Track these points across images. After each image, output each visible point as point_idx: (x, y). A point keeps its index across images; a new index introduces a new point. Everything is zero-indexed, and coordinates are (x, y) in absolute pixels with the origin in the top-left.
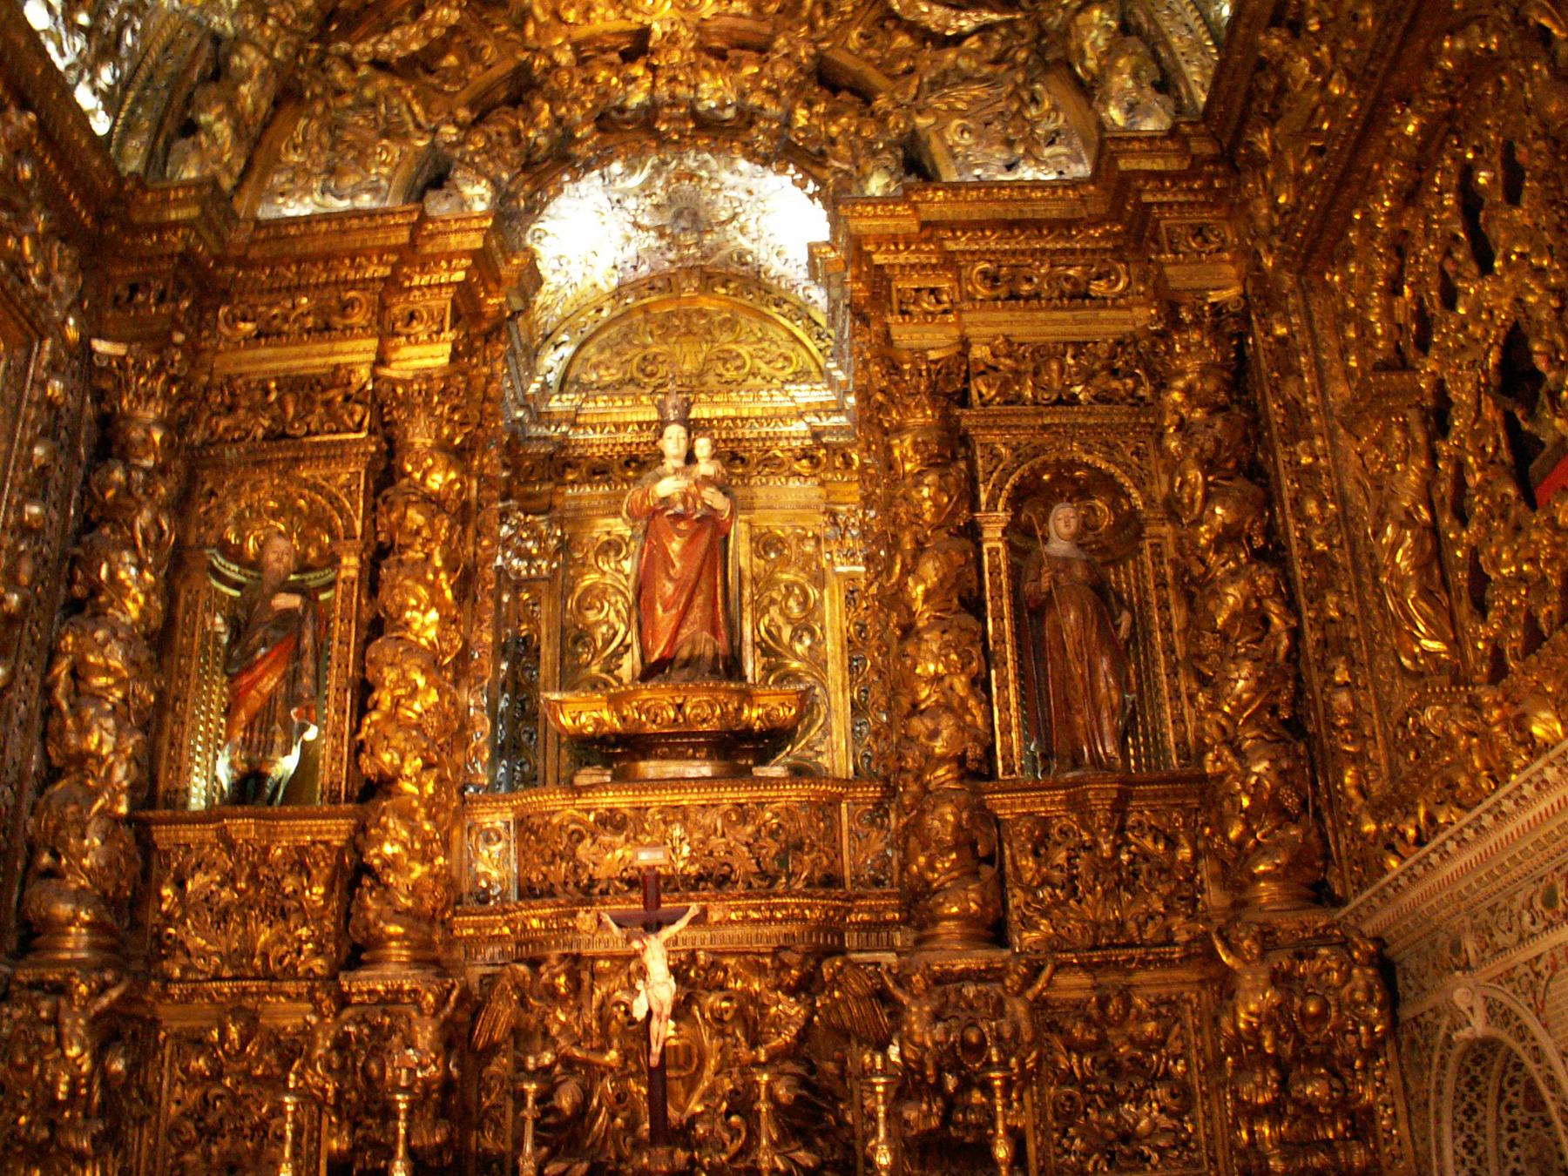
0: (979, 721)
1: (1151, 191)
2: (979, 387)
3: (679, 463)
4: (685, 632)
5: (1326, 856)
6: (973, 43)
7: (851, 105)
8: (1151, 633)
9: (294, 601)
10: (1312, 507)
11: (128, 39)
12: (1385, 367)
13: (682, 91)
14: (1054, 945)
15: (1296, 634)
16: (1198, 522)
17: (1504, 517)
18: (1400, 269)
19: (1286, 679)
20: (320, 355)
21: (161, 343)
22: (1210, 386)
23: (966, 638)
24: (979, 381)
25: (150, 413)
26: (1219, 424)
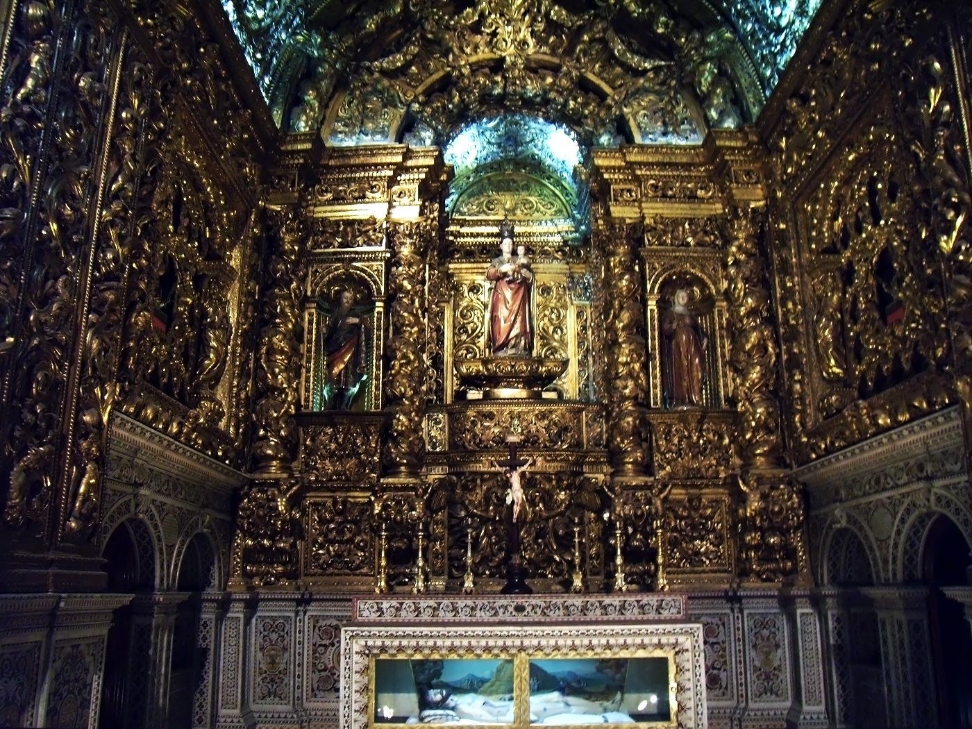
1: (730, 155)
2: (648, 238)
3: (509, 256)
5: (785, 447)
6: (651, 75)
7: (594, 100)
8: (716, 348)
9: (356, 320)
10: (790, 305)
12: (825, 251)
13: (519, 89)
14: (671, 476)
15: (778, 356)
16: (741, 305)
17: (873, 324)
18: (839, 210)
19: (772, 374)
22: (749, 246)
26: (752, 263)
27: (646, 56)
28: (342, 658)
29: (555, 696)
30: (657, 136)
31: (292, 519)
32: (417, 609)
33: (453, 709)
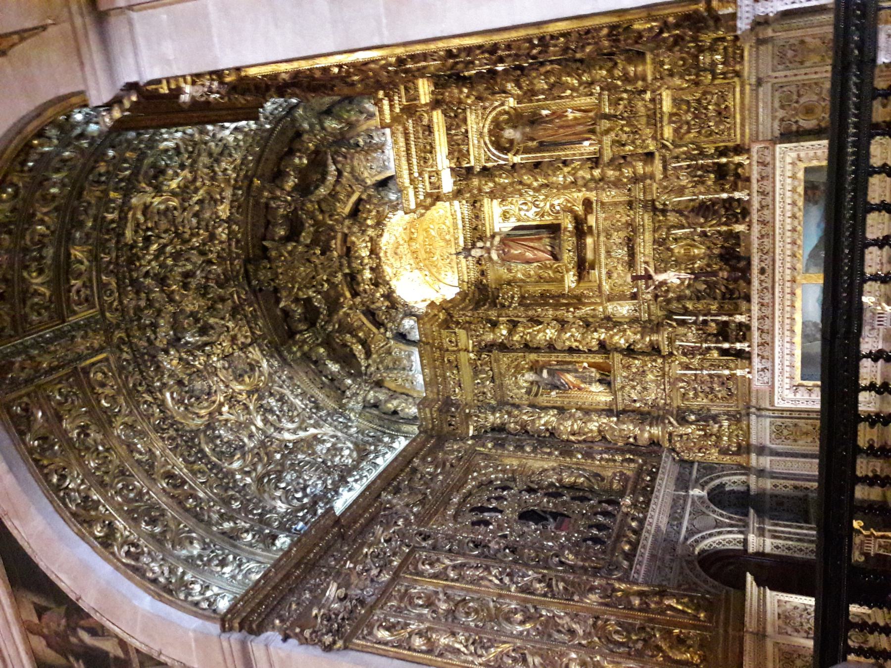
7: (365, 206)
11: (372, 434)
14: (654, 138)
15: (552, 62)
21: (469, 416)
22: (466, 90)
25: (491, 418)
27: (325, 165)
30: (385, 158)
32: (762, 344)
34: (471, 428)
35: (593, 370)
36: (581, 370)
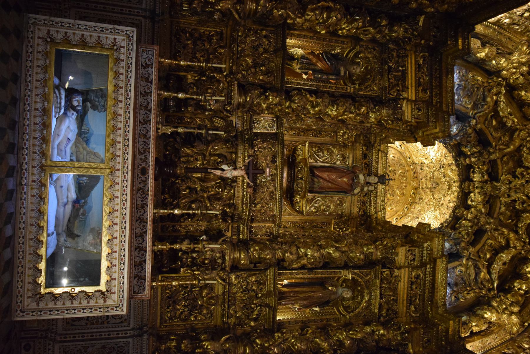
0: (294, 266)
2: (387, 272)
4: (321, 180)
14: (230, 284)
20: (411, 83)
23: (317, 264)
24: (388, 272)
26: (374, 344)
28: (111, 26)
29: (73, 195)
31: (212, 14)
33: (65, 114)
34: (421, 23)
35: (298, 71)
36: (311, 72)
